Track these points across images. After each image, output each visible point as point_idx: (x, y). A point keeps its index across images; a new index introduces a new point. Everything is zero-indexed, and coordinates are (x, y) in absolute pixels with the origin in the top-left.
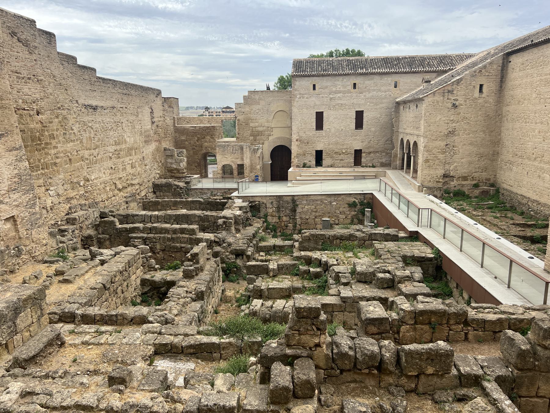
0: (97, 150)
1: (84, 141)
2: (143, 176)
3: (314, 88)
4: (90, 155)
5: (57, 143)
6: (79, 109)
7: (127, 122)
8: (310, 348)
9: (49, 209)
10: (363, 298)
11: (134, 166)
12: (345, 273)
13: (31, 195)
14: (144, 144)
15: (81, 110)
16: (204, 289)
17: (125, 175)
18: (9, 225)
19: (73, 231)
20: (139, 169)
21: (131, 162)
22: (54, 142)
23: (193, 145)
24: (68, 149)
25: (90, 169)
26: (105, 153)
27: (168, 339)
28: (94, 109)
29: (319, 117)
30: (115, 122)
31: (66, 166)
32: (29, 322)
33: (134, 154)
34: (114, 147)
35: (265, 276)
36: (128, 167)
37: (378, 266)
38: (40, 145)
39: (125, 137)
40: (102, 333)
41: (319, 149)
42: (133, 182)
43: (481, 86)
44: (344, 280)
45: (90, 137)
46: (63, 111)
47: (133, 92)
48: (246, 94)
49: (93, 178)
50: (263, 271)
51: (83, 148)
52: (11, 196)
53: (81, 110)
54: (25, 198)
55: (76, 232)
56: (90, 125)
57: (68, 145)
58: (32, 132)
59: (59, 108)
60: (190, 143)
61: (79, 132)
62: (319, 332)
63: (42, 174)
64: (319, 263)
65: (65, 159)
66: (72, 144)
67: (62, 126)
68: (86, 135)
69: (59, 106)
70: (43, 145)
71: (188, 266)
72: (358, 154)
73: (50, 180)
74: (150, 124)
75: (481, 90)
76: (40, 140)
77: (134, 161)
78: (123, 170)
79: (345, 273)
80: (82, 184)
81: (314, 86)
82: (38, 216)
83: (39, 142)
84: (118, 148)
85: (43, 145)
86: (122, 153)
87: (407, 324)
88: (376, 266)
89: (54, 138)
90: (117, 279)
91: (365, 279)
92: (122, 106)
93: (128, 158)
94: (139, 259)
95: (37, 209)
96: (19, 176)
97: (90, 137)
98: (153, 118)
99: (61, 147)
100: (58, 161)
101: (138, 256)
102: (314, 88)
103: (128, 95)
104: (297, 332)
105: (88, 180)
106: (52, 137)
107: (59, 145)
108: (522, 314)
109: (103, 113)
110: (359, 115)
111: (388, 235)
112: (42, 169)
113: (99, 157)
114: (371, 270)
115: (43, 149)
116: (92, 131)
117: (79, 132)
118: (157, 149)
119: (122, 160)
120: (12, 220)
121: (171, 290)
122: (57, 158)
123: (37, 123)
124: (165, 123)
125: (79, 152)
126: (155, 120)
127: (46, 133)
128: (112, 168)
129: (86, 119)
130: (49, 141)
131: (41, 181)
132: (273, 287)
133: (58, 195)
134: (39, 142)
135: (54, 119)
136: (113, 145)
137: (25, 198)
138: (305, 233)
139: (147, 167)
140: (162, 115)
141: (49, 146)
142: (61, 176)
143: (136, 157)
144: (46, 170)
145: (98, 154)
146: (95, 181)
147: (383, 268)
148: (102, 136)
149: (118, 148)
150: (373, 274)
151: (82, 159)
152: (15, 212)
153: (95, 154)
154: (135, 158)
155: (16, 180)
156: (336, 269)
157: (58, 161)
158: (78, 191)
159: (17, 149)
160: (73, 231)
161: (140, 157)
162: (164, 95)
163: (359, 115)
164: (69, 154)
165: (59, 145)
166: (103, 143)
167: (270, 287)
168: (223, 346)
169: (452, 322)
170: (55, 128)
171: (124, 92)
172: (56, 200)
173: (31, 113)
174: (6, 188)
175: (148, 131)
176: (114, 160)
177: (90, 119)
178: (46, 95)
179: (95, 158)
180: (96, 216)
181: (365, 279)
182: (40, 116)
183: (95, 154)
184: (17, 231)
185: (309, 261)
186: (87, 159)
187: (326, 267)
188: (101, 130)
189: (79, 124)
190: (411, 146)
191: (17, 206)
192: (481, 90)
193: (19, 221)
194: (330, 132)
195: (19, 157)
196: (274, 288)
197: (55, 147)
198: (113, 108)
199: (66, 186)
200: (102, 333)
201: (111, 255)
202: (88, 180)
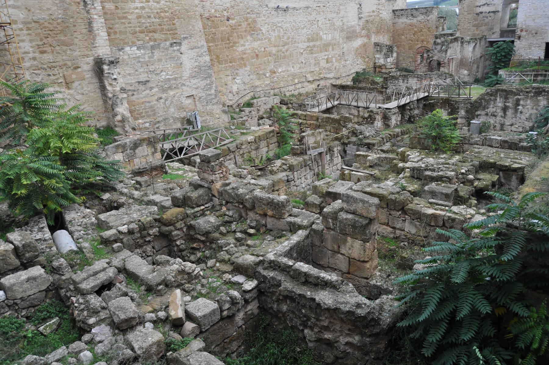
0: (286, 47)
1: (273, 39)
2: (341, 71)
4: (278, 51)
5: (244, 42)
6: (269, 12)
7: (324, 20)
9: (235, 94)
11: (329, 61)
13: (208, 82)
14: (345, 40)
15: (270, 13)
17: (317, 69)
18: (190, 101)
19: (251, 112)
20: (336, 64)
21: (326, 57)
22: (242, 42)
23: (410, 40)
24: (256, 47)
25: (277, 63)
26: (296, 50)
28: (285, 11)
30: (309, 21)
31: (253, 61)
32: (146, 154)
34: (307, 44)
36: (323, 63)
38: (229, 43)
39: (321, 34)
42: (328, 76)
45: (279, 36)
46: (252, 16)
49: (280, 70)
51: (271, 45)
52: (192, 81)
53: (270, 13)
54: (203, 84)
56: (280, 25)
57: (256, 43)
58: (222, 34)
59: (249, 13)
60: (406, 38)
61: (268, 31)
62: (211, 173)
63: (230, 66)
65: (252, 54)
66: (259, 42)
67: (251, 27)
69: (248, 11)
70: (231, 44)
73: (237, 71)
74: (356, 19)
76: (229, 40)
77: (330, 56)
78: (315, 65)
80: (267, 75)
82: (213, 97)
83: (228, 42)
84: (311, 44)
85: (231, 44)
86: (315, 49)
89: (242, 38)
90: (243, 147)
92: (319, 5)
93: (323, 54)
94: (273, 136)
95: (213, 91)
96: (199, 67)
97: (279, 36)
100: (245, 56)
101: (271, 134)
105: (275, 73)
106: (240, 37)
107: (247, 44)
109: (295, 14)
111: (506, 142)
112: (230, 62)
113: (288, 53)
115: (232, 46)
116: (281, 30)
117: (268, 31)
118: (364, 45)
120: (192, 97)
122: (245, 54)
123: (227, 27)
124: (378, 18)
125: (266, 49)
127: (235, 34)
129: (275, 20)
130: (237, 40)
131: (228, 72)
133: (244, 83)
134: (228, 42)
135: (243, 22)
136: (304, 42)
137: (203, 84)
139: (348, 62)
140: (375, 9)
141: (237, 45)
142: (248, 68)
143: (333, 52)
144: (234, 64)
145: (287, 51)
146: (282, 73)
148: (292, 34)
149: (311, 44)
151: (270, 54)
152: (194, 93)
153: (284, 50)
154: (331, 53)
155: (196, 70)
157: (245, 56)
158: (264, 81)
159: (199, 48)
160: (251, 112)
161: (337, 52)
164: (256, 51)
165: (247, 44)
166: (294, 40)
170: (244, 29)
172: (242, 87)
173: (222, 19)
174: (188, 76)
175: (352, 27)
176: (305, 55)
177: (280, 20)
178: (236, 3)
179: (283, 54)
180: (275, 102)
182: (231, 21)
183: (284, 50)
184: (196, 106)
188: (292, 29)
189: (268, 25)
191: (196, 88)
193: (197, 99)
195: (200, 54)
197: (244, 45)
198: (307, 8)
199: (251, 77)
202: (275, 73)
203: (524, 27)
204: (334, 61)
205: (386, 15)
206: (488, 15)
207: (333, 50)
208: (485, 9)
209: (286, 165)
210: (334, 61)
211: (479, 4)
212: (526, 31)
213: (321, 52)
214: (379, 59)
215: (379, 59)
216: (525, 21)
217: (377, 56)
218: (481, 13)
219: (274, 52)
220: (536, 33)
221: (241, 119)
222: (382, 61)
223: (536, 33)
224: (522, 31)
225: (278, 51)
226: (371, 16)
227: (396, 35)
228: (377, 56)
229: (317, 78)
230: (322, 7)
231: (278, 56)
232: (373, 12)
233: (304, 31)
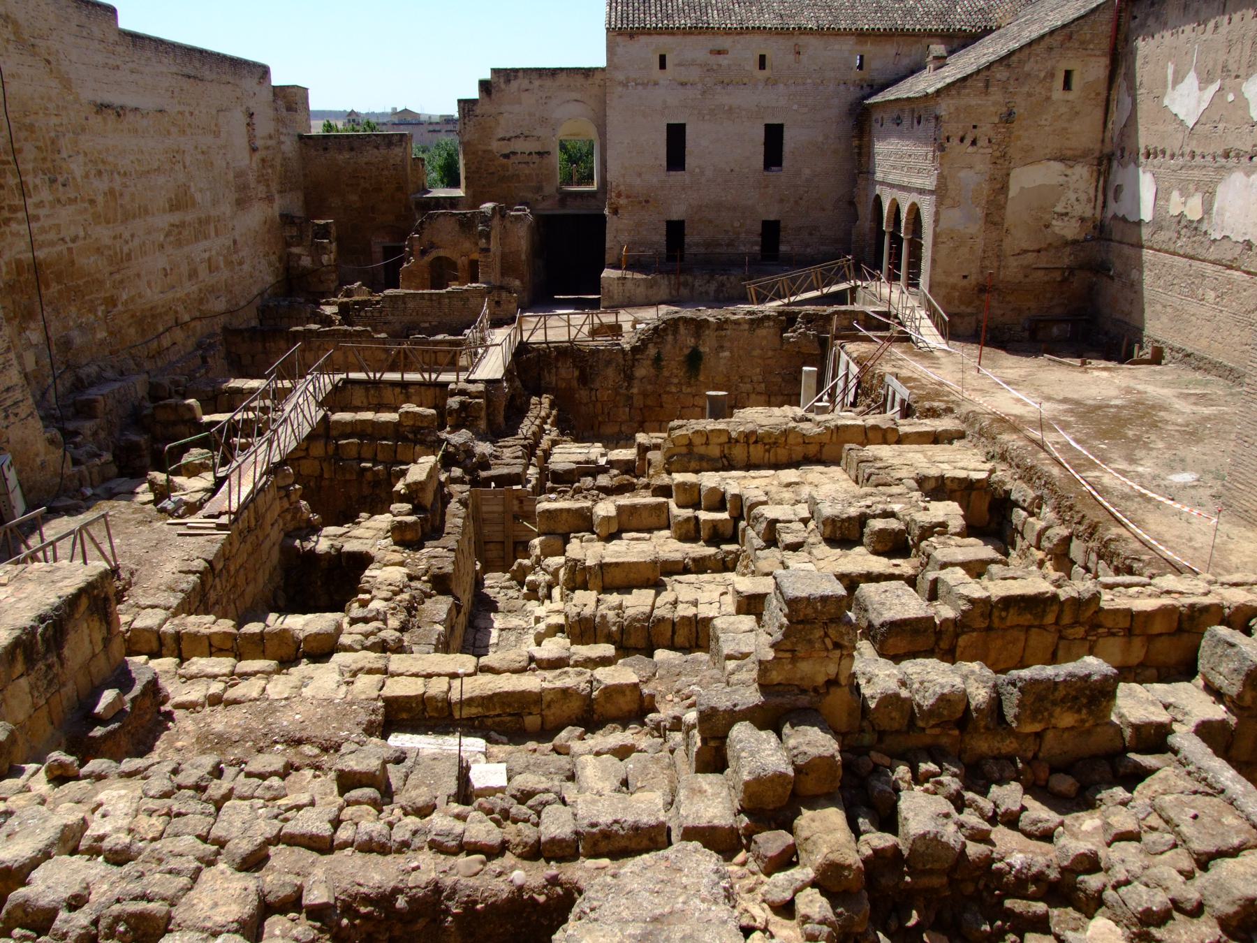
1: (100, 199)
3: (663, 65)
8: (815, 690)
10: (871, 578)
12: (790, 522)
16: (449, 569)
21: (206, 255)
27: (401, 688)
29: (676, 135)
33: (213, 234)
35: (587, 535)
37: (869, 503)
39: (193, 190)
40: (245, 676)
41: (675, 218)
43: (1068, 74)
44: (788, 538)
45: (112, 192)
47: (207, 74)
48: (487, 76)
50: (583, 522)
55: (102, 435)
64: (719, 501)
68: (101, 185)
71: (400, 514)
72: (771, 230)
74: (246, 154)
75: (1067, 85)
77: (214, 253)
78: (190, 277)
79: (790, 522)
81: (663, 60)
84: (176, 218)
87: (974, 630)
88: (863, 503)
91: (843, 533)
92: (181, 108)
97: (112, 192)
98: (251, 138)
99: (47, 216)
102: (663, 65)
103: (195, 77)
104: (788, 655)
108: (1206, 594)
110: (774, 135)
111: (875, 428)
113: (136, 242)
114: (853, 511)
119: (186, 249)
121: (367, 573)
126: (259, 143)
128: (165, 269)
132: (614, 560)
136: (164, 211)
138: (680, 427)
147: (880, 506)
149: (176, 218)
150: (862, 519)
156: (770, 512)
162: (277, 79)
163: (774, 135)
167: (607, 560)
168: (549, 698)
169: (1066, 620)
171: (186, 71)
181: (843, 533)
183: (127, 235)
185: (692, 497)
186: (109, 248)
187: (740, 508)
190: (903, 216)
192: (1067, 85)
194: (702, 173)
196: (617, 564)
200: (245, 676)
201: (206, 490)
203: (622, 188)
204: (222, 265)
205: (289, 146)
206: (527, 159)
207: (217, 235)
208: (520, 146)
209: (418, 579)
210: (222, 265)
211: (508, 136)
212: (628, 197)
213: (197, 240)
214: (299, 256)
215: (299, 256)
216: (624, 176)
217: (295, 250)
218: (514, 153)
219: (107, 241)
220: (647, 202)
221: (97, 461)
222: (306, 261)
223: (647, 202)
224: (619, 195)
225: (115, 238)
226: (267, 148)
227: (315, 200)
228: (295, 250)
229: (198, 314)
230: (187, 114)
231: (116, 253)
232: (270, 137)
233: (161, 180)
